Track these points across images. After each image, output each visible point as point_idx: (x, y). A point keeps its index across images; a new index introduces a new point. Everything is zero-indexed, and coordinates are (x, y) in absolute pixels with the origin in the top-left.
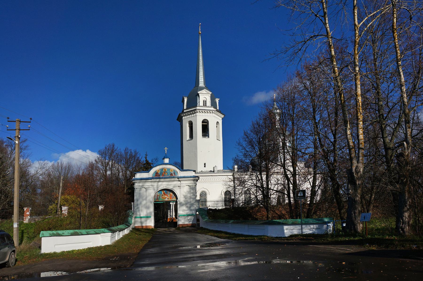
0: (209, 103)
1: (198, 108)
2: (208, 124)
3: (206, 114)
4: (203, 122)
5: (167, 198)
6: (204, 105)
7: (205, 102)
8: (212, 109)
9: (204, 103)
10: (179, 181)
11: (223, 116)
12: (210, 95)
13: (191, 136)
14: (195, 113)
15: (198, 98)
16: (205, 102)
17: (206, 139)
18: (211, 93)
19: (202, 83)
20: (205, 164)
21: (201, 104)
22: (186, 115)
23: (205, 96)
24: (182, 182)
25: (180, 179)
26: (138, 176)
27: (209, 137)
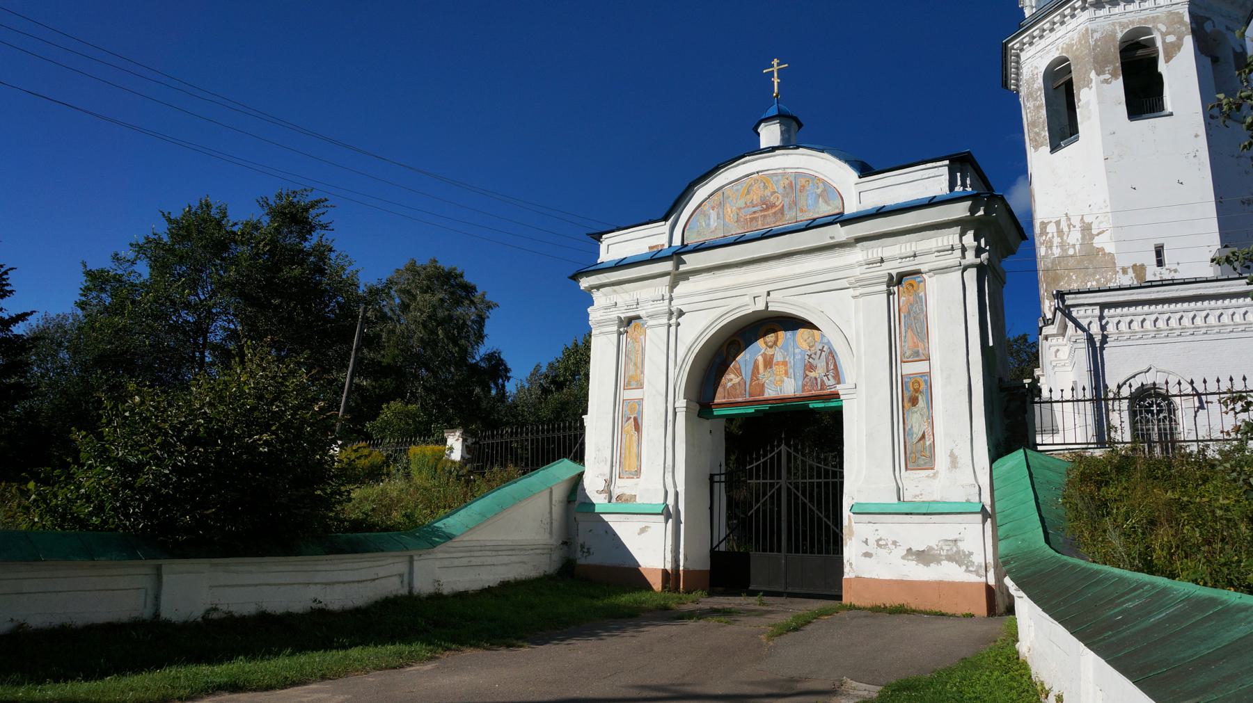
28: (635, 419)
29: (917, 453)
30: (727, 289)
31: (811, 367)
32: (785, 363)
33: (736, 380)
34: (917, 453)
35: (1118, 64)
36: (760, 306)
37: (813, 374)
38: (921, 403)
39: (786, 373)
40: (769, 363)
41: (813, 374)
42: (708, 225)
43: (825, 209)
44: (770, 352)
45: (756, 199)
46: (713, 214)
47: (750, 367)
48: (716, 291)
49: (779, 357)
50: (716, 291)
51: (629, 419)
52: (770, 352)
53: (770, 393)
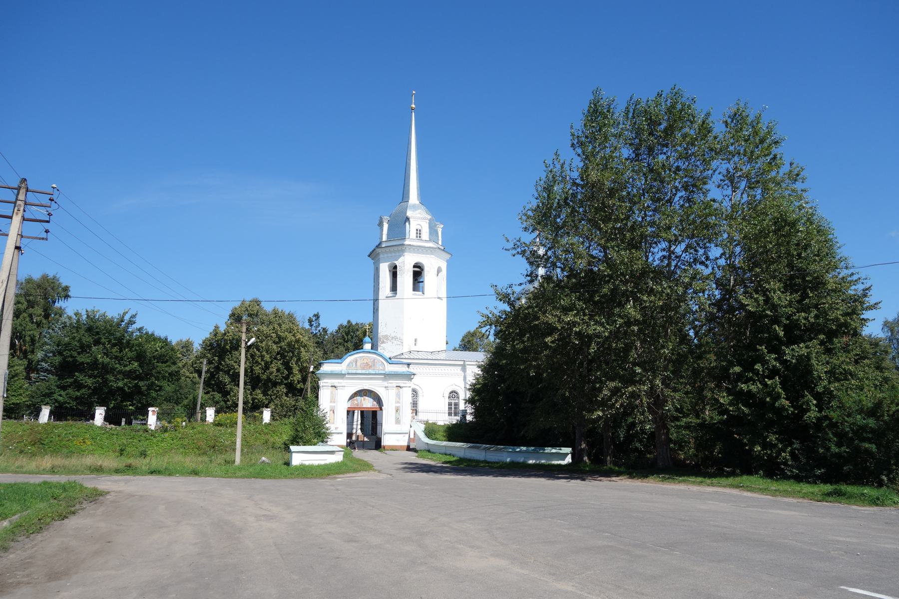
0: (425, 235)
1: (407, 242)
2: (422, 270)
4: (414, 267)
5: (368, 403)
7: (419, 232)
8: (431, 245)
11: (448, 256)
13: (394, 288)
16: (419, 232)
18: (429, 217)
20: (416, 340)
21: (413, 234)
22: (386, 252)
23: (419, 220)
26: (327, 367)
29: (398, 421)
34: (398, 421)
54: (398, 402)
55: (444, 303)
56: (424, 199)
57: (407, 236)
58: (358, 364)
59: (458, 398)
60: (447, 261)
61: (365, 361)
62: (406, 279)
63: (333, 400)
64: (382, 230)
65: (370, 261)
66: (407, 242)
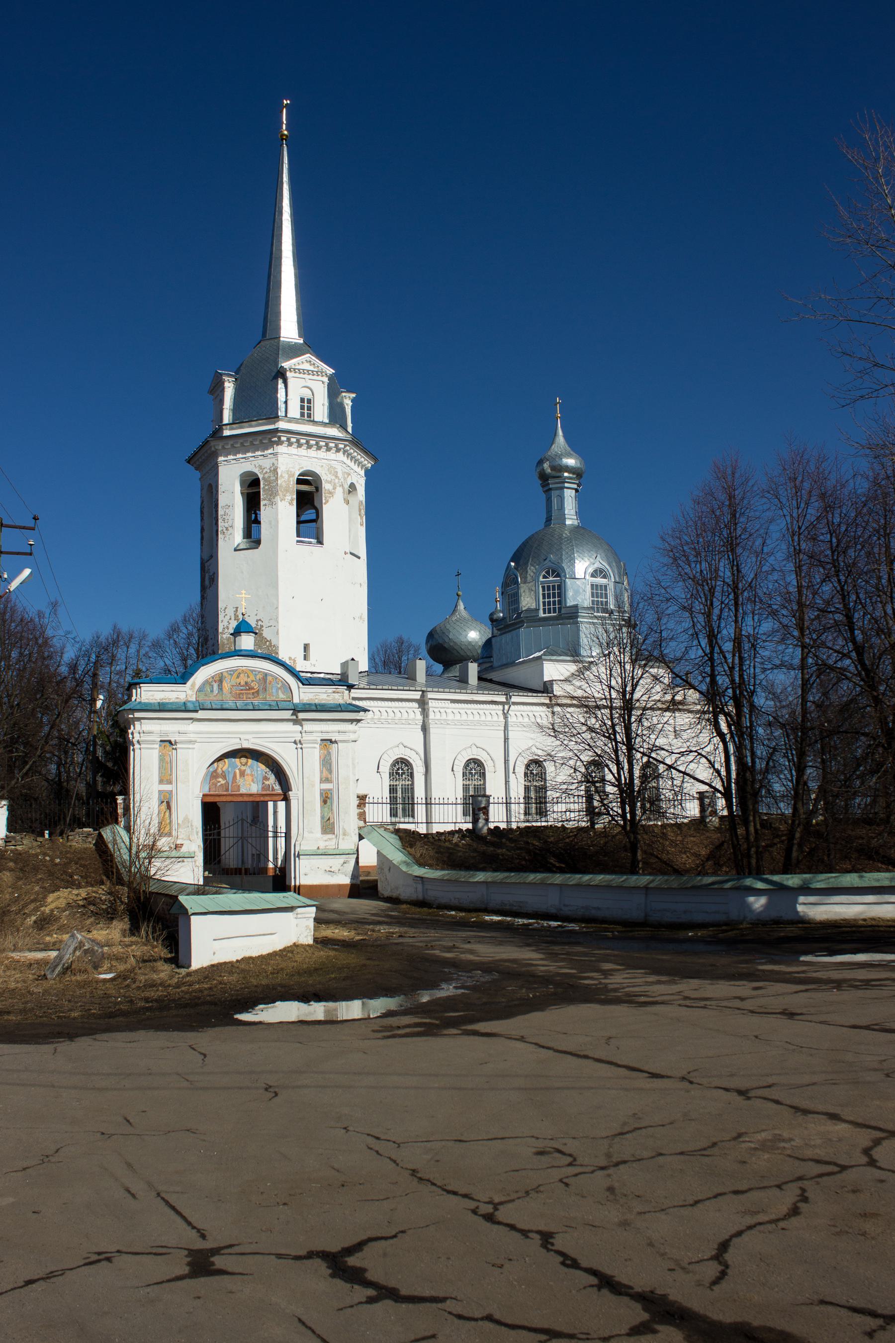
0: (321, 411)
2: (318, 489)
3: (312, 452)
4: (299, 482)
5: (252, 781)
6: (302, 415)
7: (306, 405)
8: (334, 432)
9: (302, 408)
10: (297, 722)
12: (326, 380)
14: (271, 444)
15: (281, 385)
16: (306, 405)
17: (310, 550)
18: (331, 371)
19: (289, 329)
21: (294, 411)
23: (306, 383)
24: (308, 726)
25: (301, 716)
26: (148, 693)
27: (320, 542)
28: (168, 803)
30: (229, 733)
31: (267, 779)
32: (252, 775)
33: (223, 782)
34: (328, 827)
35: (295, 496)
36: (246, 745)
37: (267, 783)
38: (328, 803)
39: (253, 780)
40: (242, 774)
41: (267, 783)
42: (212, 691)
43: (282, 696)
44: (243, 768)
45: (243, 683)
46: (216, 686)
47: (231, 776)
48: (222, 733)
49: (248, 771)
50: (222, 733)
51: (162, 802)
52: (243, 768)
53: (243, 791)
54: (327, 780)
55: (361, 566)
56: (315, 339)
57: (281, 413)
58: (226, 686)
59: (412, 775)
60: (368, 473)
61: (243, 680)
62: (281, 513)
63: (166, 777)
64: (221, 402)
65: (193, 475)
66: (282, 425)
